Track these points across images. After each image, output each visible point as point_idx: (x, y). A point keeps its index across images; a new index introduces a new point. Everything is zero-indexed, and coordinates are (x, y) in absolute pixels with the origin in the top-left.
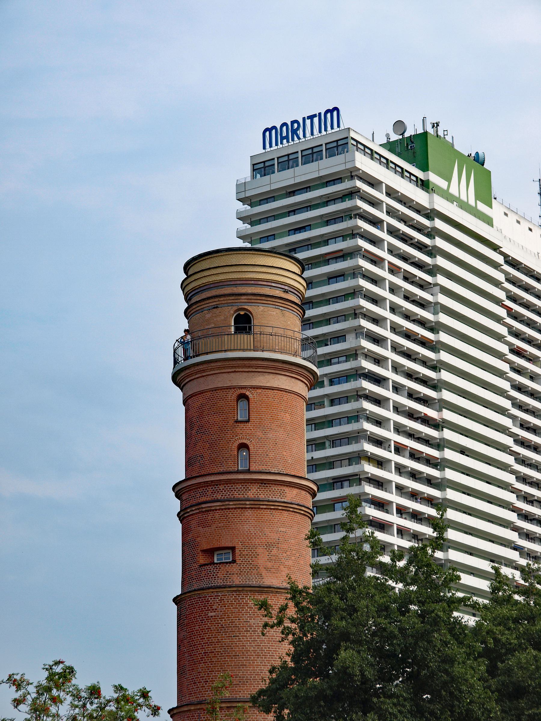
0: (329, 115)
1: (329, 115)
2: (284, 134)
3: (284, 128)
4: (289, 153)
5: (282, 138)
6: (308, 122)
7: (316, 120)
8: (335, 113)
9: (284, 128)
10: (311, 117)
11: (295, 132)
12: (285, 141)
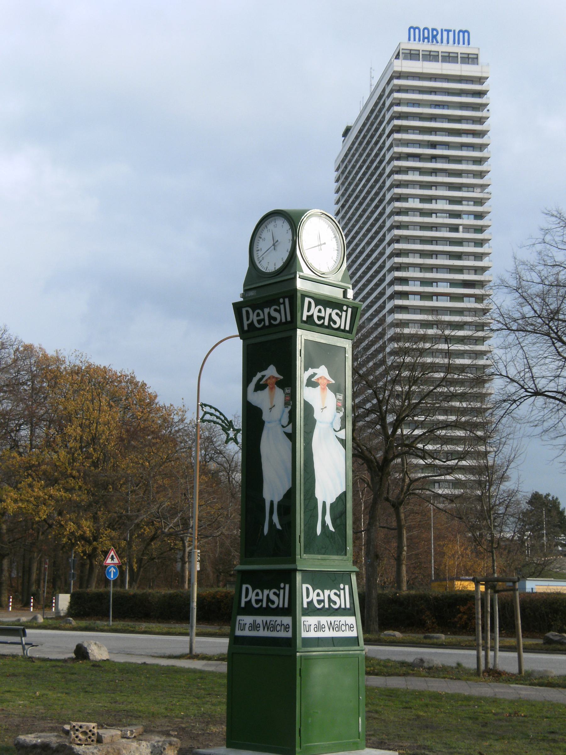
0: (461, 34)
1: (461, 34)
2: (426, 35)
3: (426, 31)
4: (433, 50)
5: (424, 38)
6: (445, 34)
7: (451, 34)
8: (466, 34)
9: (426, 31)
10: (448, 31)
11: (434, 37)
12: (426, 40)
